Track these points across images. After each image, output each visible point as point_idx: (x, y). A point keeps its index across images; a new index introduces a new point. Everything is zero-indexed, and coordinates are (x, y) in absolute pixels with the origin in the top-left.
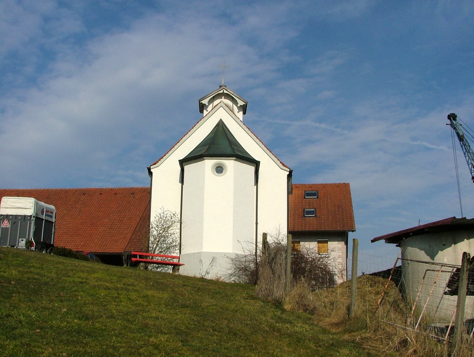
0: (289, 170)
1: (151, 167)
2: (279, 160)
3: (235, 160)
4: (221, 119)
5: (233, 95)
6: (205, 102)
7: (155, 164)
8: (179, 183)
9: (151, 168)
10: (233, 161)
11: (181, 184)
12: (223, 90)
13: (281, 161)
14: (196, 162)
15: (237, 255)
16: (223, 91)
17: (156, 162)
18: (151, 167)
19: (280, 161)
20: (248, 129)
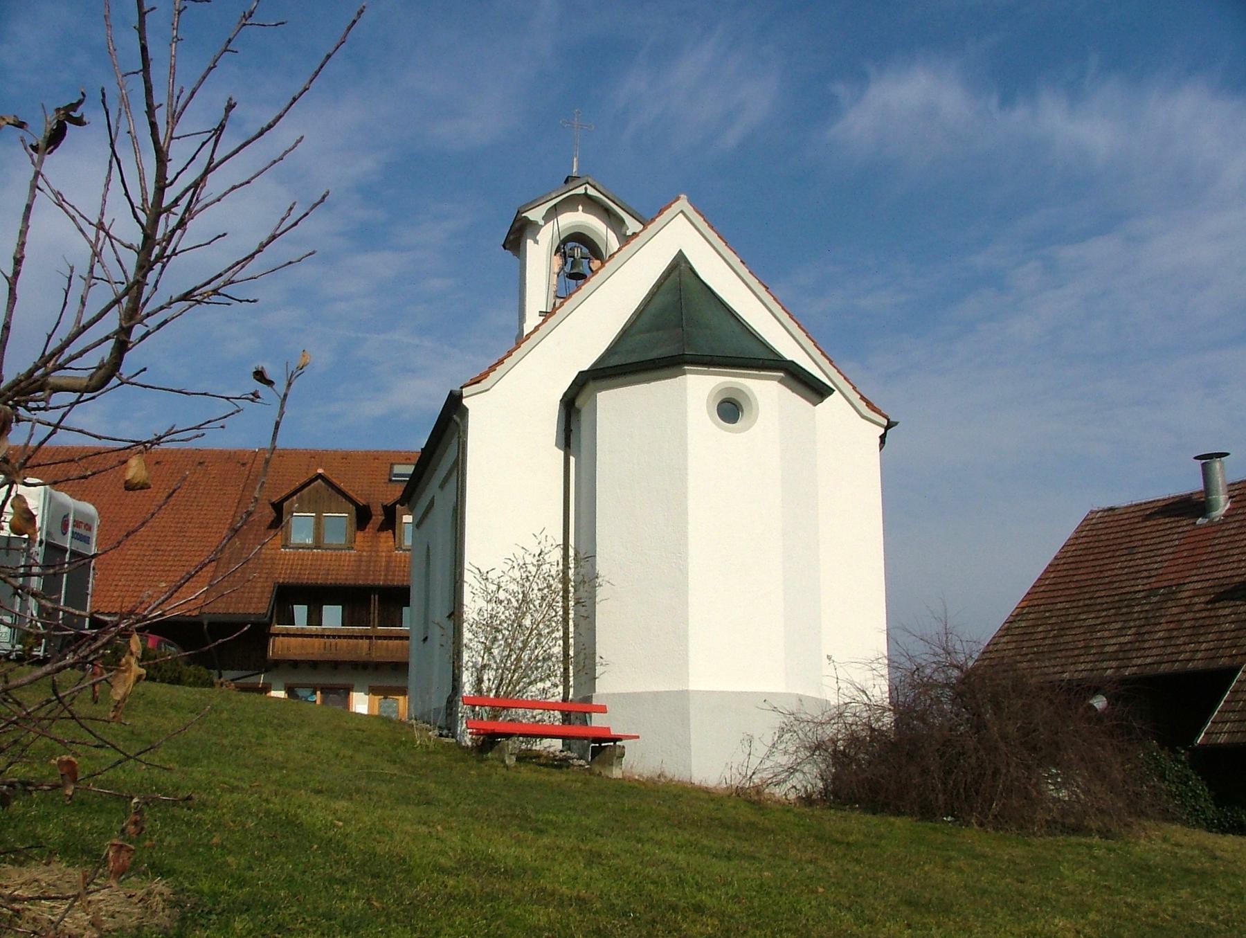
0: (885, 422)
1: (466, 391)
2: (857, 389)
3: (781, 381)
4: (680, 251)
5: (614, 202)
6: (536, 215)
7: (478, 382)
8: (556, 448)
9: (464, 395)
10: (776, 382)
11: (562, 453)
12: (584, 186)
13: (863, 394)
14: (648, 381)
15: (800, 699)
16: (586, 189)
17: (481, 375)
18: (466, 391)
19: (859, 393)
20: (764, 289)
